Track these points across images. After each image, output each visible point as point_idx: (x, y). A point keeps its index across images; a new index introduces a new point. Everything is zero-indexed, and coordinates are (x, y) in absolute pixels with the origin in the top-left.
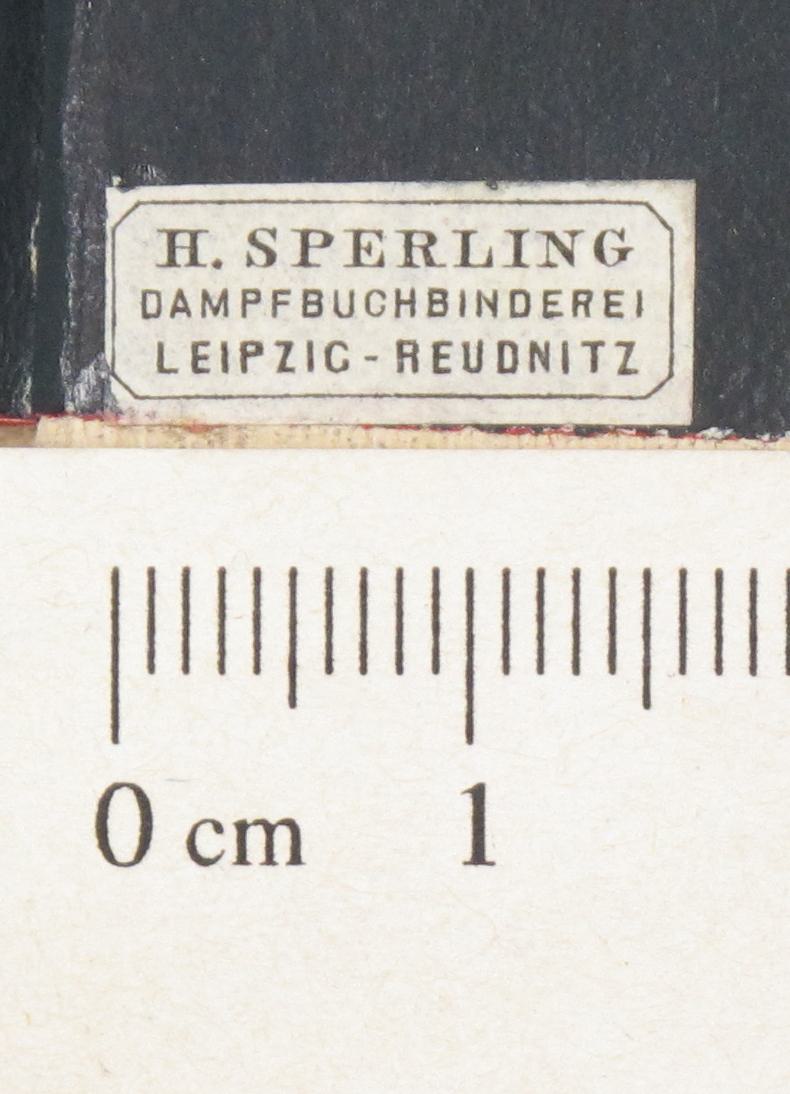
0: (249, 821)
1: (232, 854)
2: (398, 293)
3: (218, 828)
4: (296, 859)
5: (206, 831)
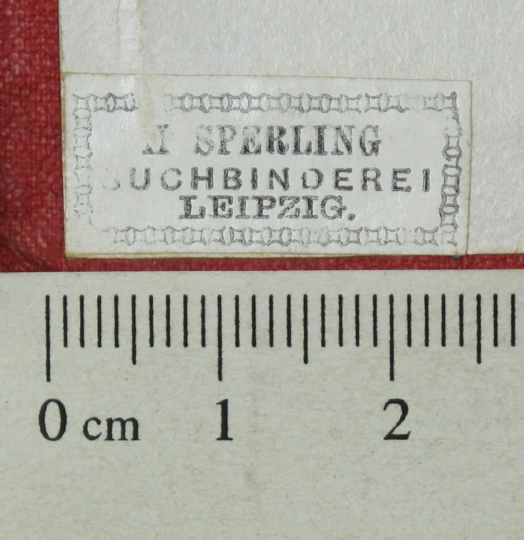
0: (113, 419)
1: (105, 434)
2: (195, 170)
3: (99, 422)
4: (136, 437)
5: (92, 425)
